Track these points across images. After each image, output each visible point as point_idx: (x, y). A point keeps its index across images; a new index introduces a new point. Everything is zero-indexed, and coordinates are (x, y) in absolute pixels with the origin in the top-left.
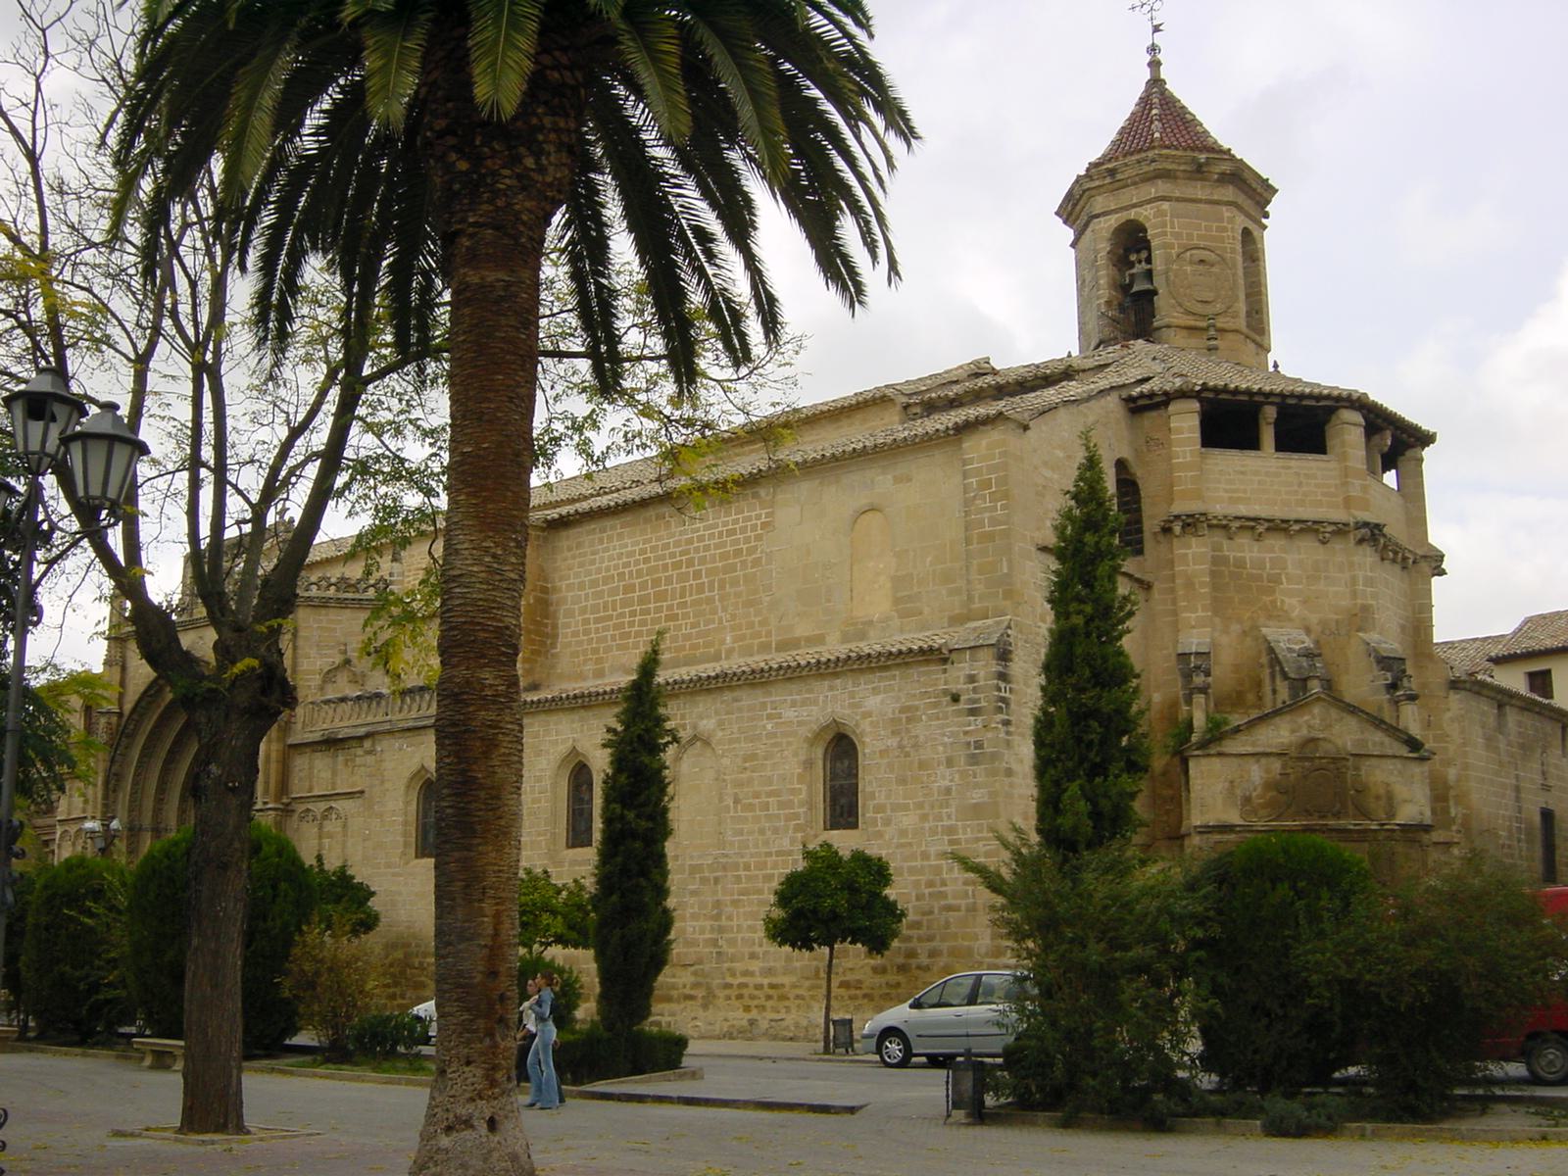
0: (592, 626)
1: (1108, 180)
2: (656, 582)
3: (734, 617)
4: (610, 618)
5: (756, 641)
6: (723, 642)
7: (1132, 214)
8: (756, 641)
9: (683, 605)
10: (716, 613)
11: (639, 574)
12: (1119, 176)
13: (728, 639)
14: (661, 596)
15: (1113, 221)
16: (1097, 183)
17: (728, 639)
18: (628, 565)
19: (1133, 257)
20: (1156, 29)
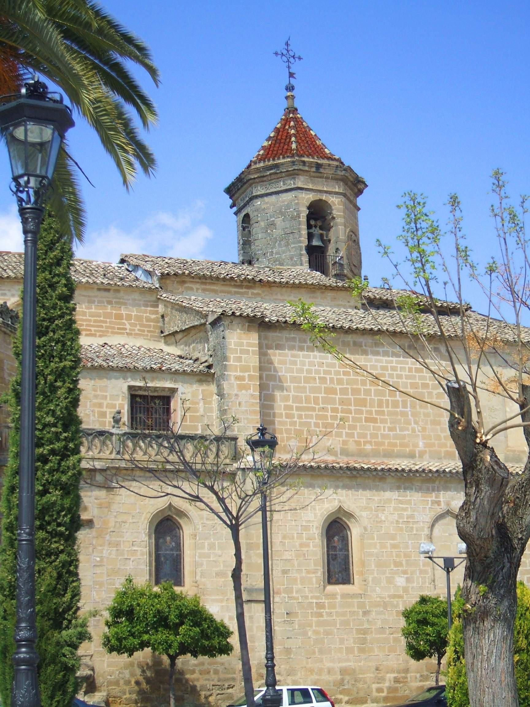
0: (329, 414)
1: (314, 169)
2: (356, 392)
3: (424, 429)
4: (314, 409)
5: (443, 450)
6: (416, 445)
7: (324, 197)
8: (443, 450)
9: (383, 413)
10: (410, 424)
11: (340, 382)
12: (322, 170)
13: (421, 444)
14: (363, 402)
15: (311, 197)
16: (306, 168)
17: (421, 444)
18: (329, 373)
19: (312, 222)
20: (291, 75)
